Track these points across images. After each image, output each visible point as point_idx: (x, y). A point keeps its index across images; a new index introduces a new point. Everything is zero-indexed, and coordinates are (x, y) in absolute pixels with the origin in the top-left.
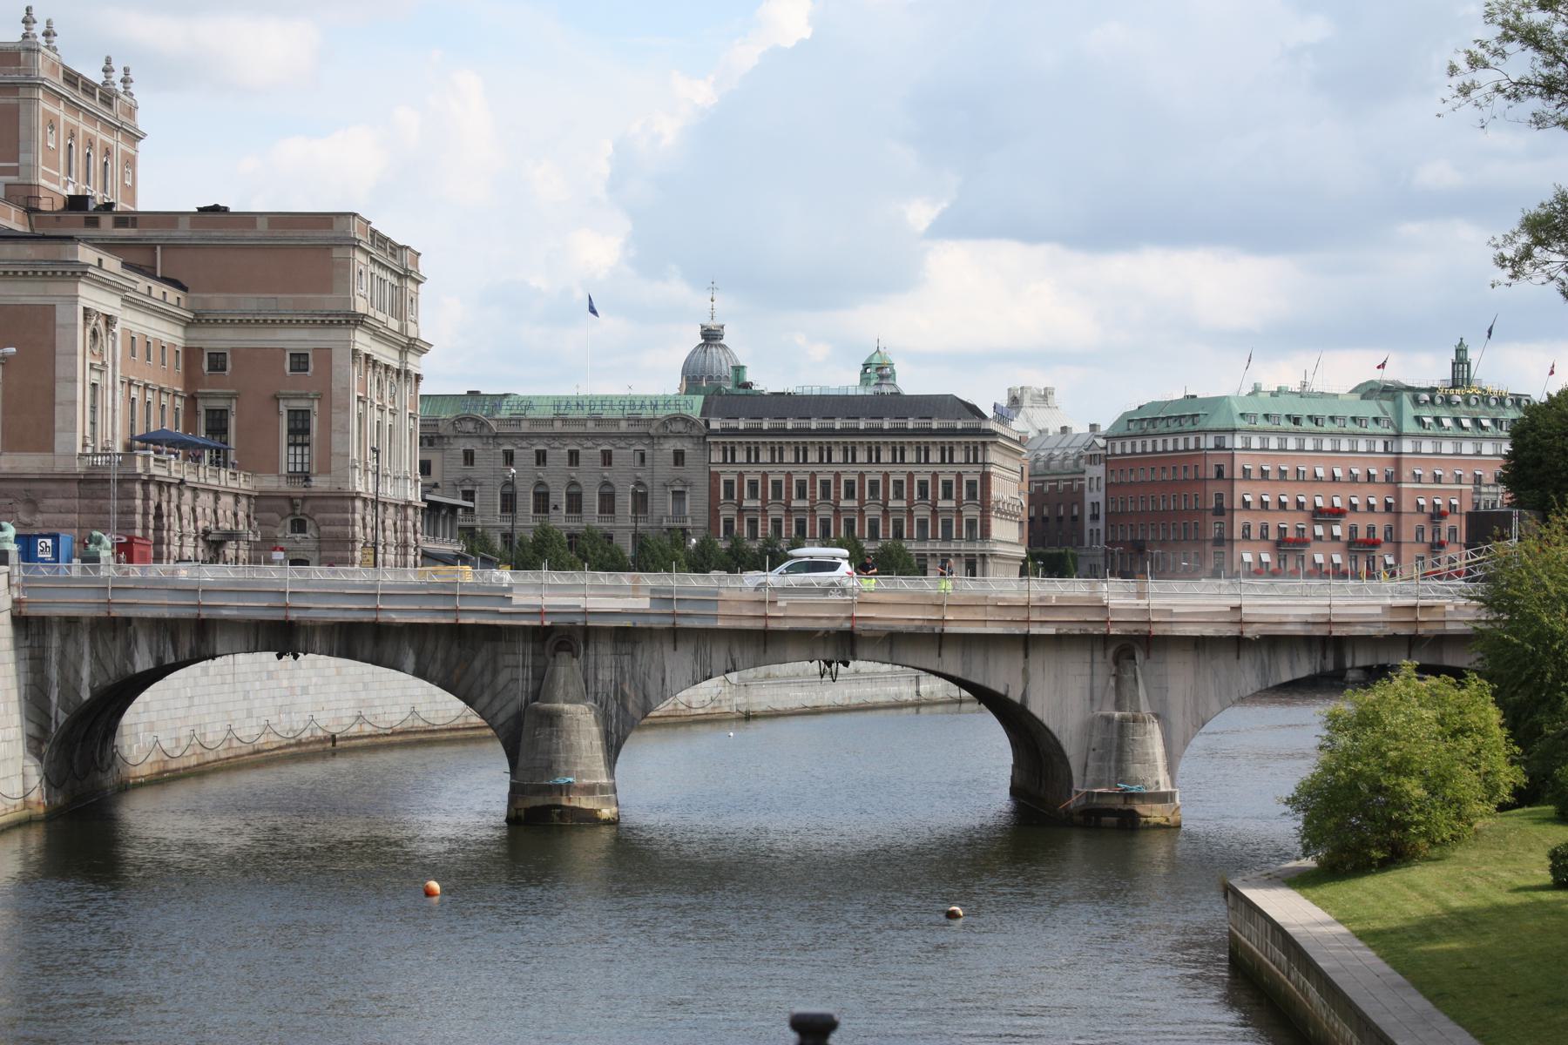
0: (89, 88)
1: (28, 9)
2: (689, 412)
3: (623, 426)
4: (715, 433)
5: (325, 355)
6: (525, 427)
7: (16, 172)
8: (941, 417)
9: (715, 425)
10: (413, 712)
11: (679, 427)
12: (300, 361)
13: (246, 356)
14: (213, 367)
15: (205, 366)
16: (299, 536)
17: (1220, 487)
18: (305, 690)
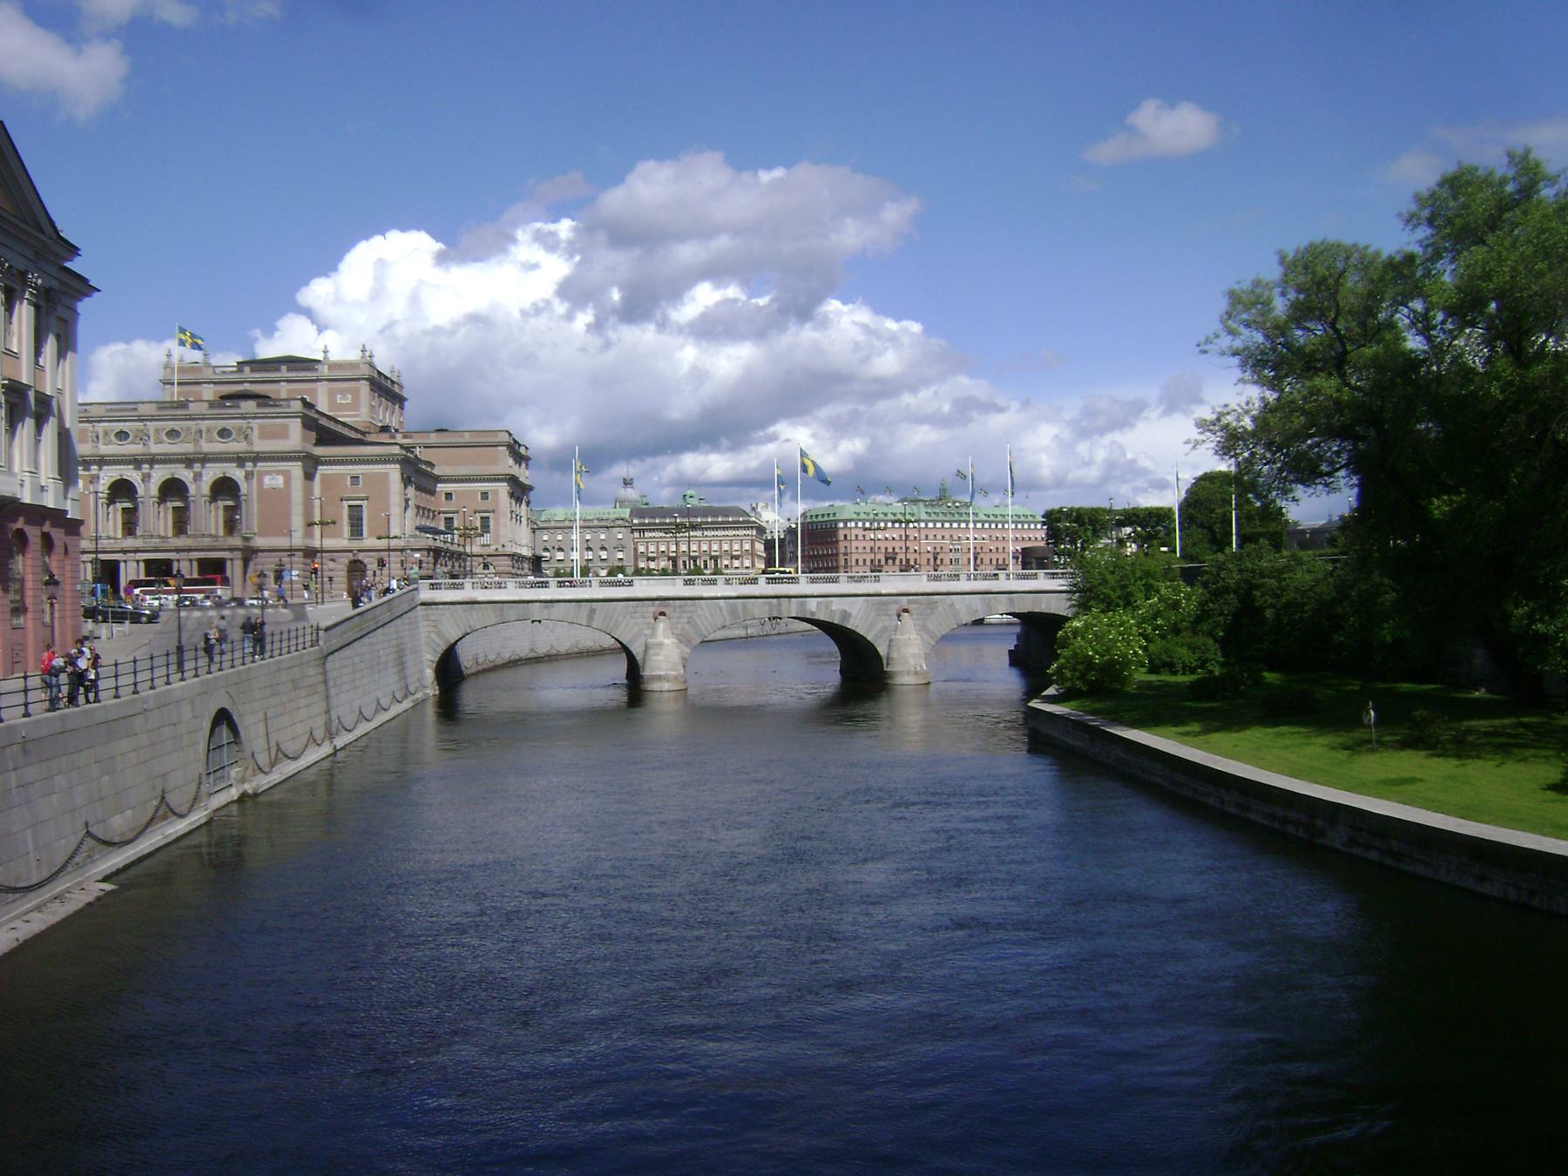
0: (386, 378)
1: (364, 346)
2: (623, 516)
3: (596, 523)
4: (635, 525)
5: (496, 492)
6: (553, 524)
7: (358, 416)
8: (733, 516)
9: (635, 521)
10: (552, 647)
11: (620, 522)
12: (485, 495)
13: (462, 494)
14: (447, 498)
15: (443, 498)
16: (486, 571)
17: (847, 544)
18: (511, 638)
